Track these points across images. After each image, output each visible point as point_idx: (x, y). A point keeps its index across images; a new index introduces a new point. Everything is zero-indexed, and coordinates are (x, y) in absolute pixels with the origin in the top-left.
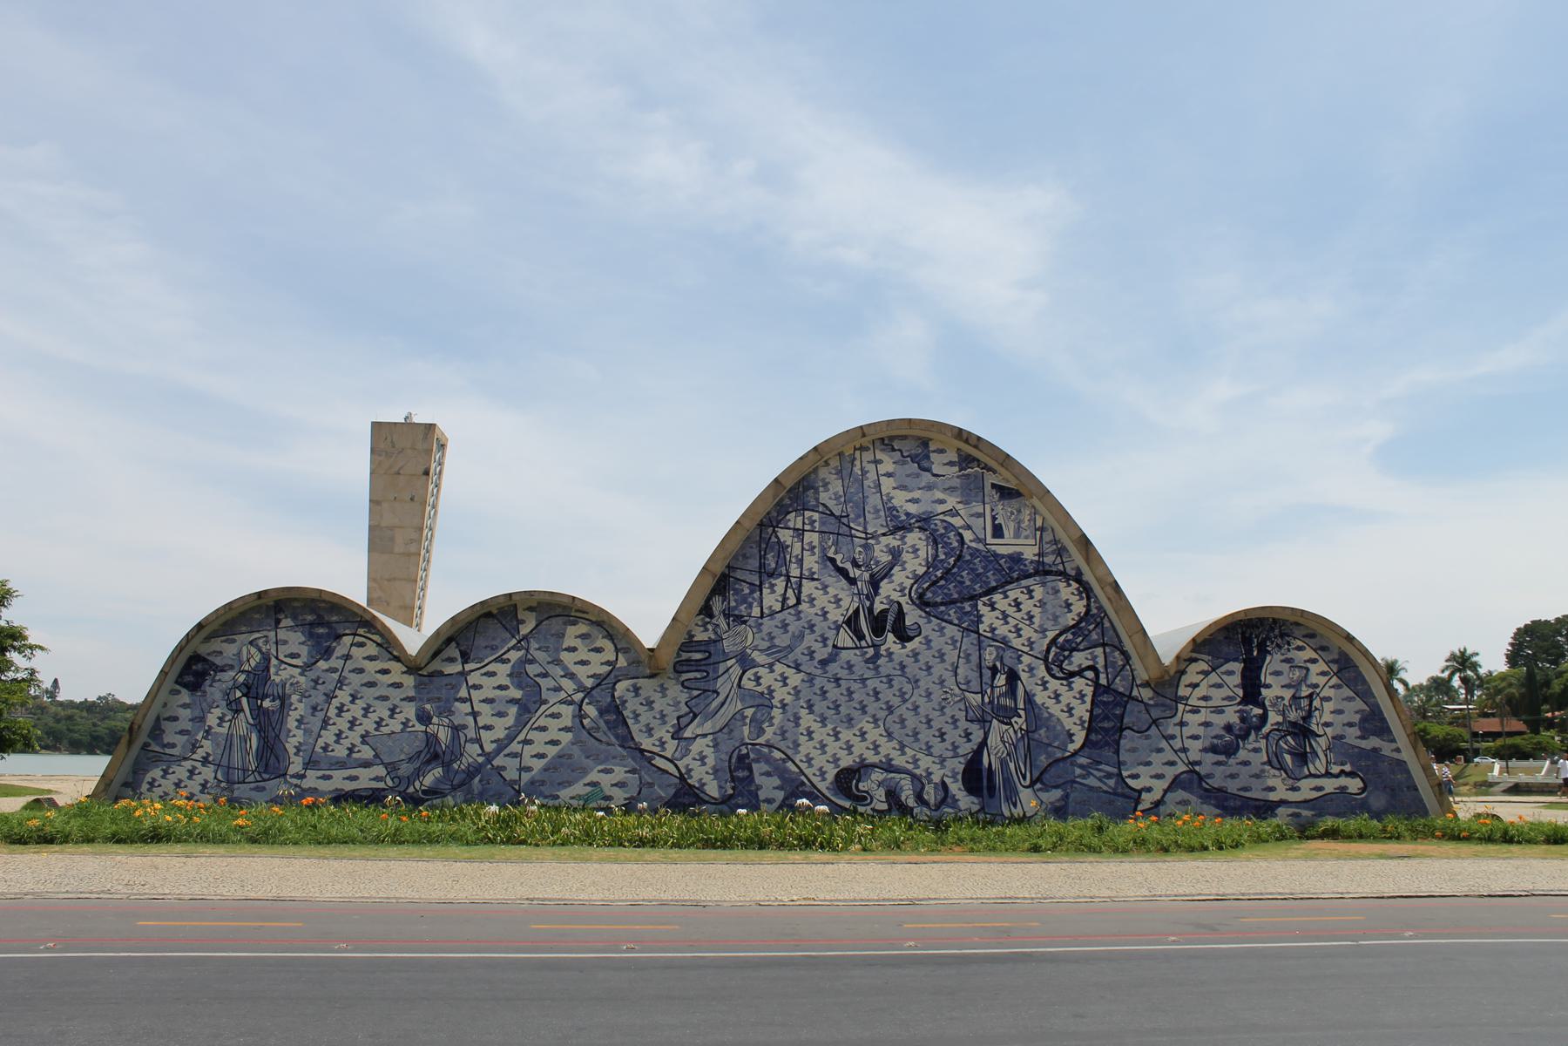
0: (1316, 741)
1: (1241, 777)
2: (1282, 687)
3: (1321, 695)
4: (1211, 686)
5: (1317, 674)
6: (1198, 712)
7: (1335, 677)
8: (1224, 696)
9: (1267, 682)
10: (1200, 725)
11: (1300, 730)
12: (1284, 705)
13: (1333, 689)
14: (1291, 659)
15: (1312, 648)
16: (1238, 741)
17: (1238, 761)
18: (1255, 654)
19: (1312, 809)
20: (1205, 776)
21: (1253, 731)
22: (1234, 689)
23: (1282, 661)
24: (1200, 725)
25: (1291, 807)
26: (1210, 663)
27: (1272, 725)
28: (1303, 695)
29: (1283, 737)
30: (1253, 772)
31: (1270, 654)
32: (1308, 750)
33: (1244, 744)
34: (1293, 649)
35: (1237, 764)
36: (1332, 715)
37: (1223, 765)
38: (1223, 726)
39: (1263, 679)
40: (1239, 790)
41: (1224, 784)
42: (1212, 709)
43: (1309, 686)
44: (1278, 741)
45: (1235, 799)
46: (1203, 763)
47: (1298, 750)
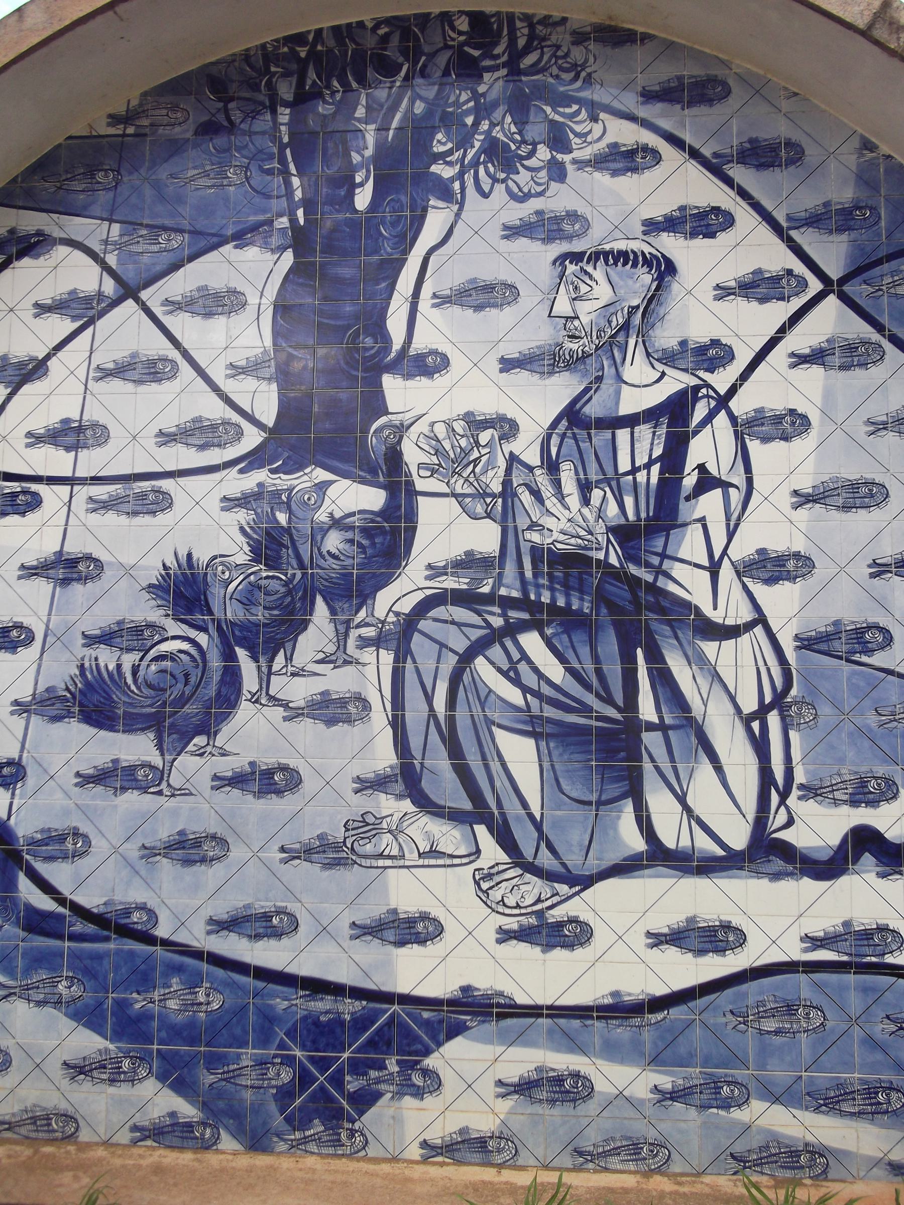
0: (699, 661)
1: (238, 853)
2: (508, 365)
3: (741, 405)
4: (105, 374)
5: (723, 292)
6: (35, 502)
7: (832, 299)
8: (170, 422)
9: (419, 344)
10: (31, 572)
11: (602, 598)
12: (513, 459)
13: (816, 371)
14: (573, 216)
15: (694, 154)
16: (229, 656)
17: (226, 766)
18: (363, 199)
19: (656, 1061)
20: (33, 842)
21: (320, 607)
22: (229, 386)
23: (513, 232)
24: (31, 572)
25: (518, 1039)
26: (112, 260)
27: (435, 572)
28: (625, 409)
29: (493, 637)
30: (308, 834)
31: (446, 194)
32: (647, 710)
33: (266, 678)
34: (580, 164)
35: (222, 782)
36: (803, 513)
37: (144, 790)
38: (153, 576)
39: (396, 325)
40: (220, 926)
41: (137, 894)
42: (101, 492)
43: (669, 358)
44: (467, 658)
45: (193, 984)
46: (31, 780)
47: (585, 709)
